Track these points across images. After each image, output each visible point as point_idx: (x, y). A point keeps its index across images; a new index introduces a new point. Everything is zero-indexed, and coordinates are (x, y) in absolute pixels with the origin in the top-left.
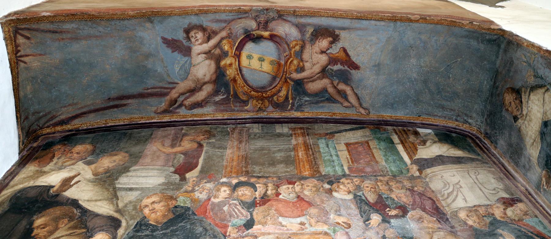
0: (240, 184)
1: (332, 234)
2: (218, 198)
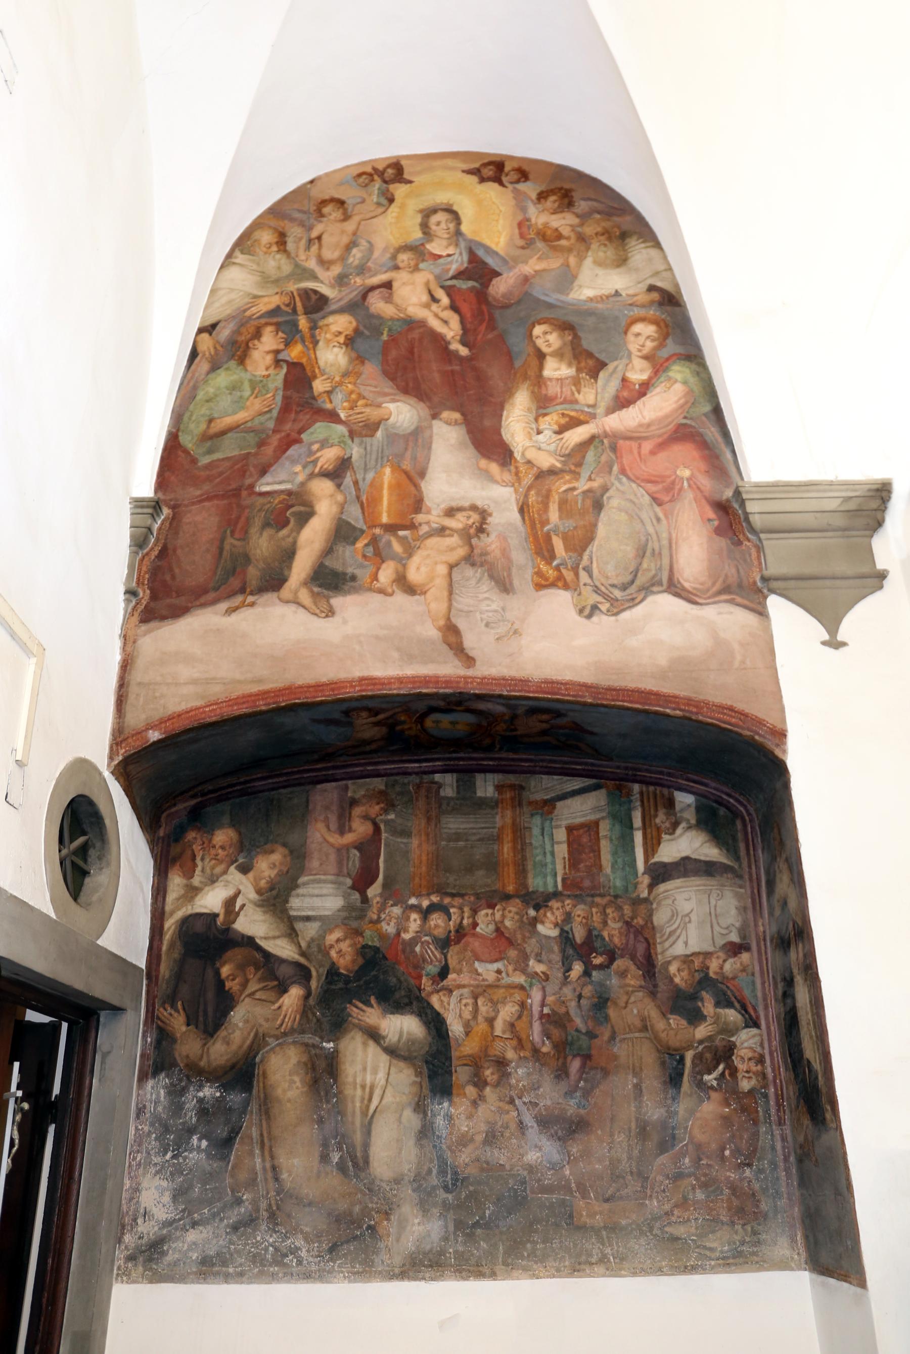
0: (432, 908)
1: (528, 988)
2: (408, 932)
